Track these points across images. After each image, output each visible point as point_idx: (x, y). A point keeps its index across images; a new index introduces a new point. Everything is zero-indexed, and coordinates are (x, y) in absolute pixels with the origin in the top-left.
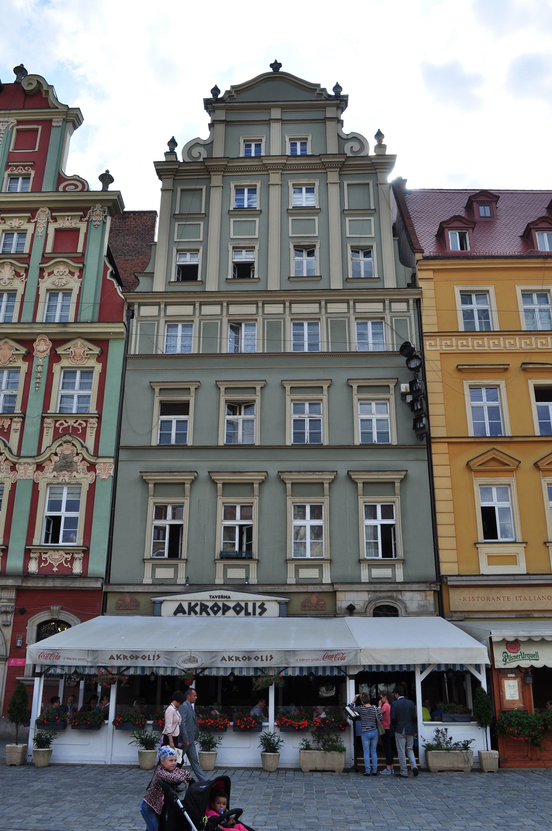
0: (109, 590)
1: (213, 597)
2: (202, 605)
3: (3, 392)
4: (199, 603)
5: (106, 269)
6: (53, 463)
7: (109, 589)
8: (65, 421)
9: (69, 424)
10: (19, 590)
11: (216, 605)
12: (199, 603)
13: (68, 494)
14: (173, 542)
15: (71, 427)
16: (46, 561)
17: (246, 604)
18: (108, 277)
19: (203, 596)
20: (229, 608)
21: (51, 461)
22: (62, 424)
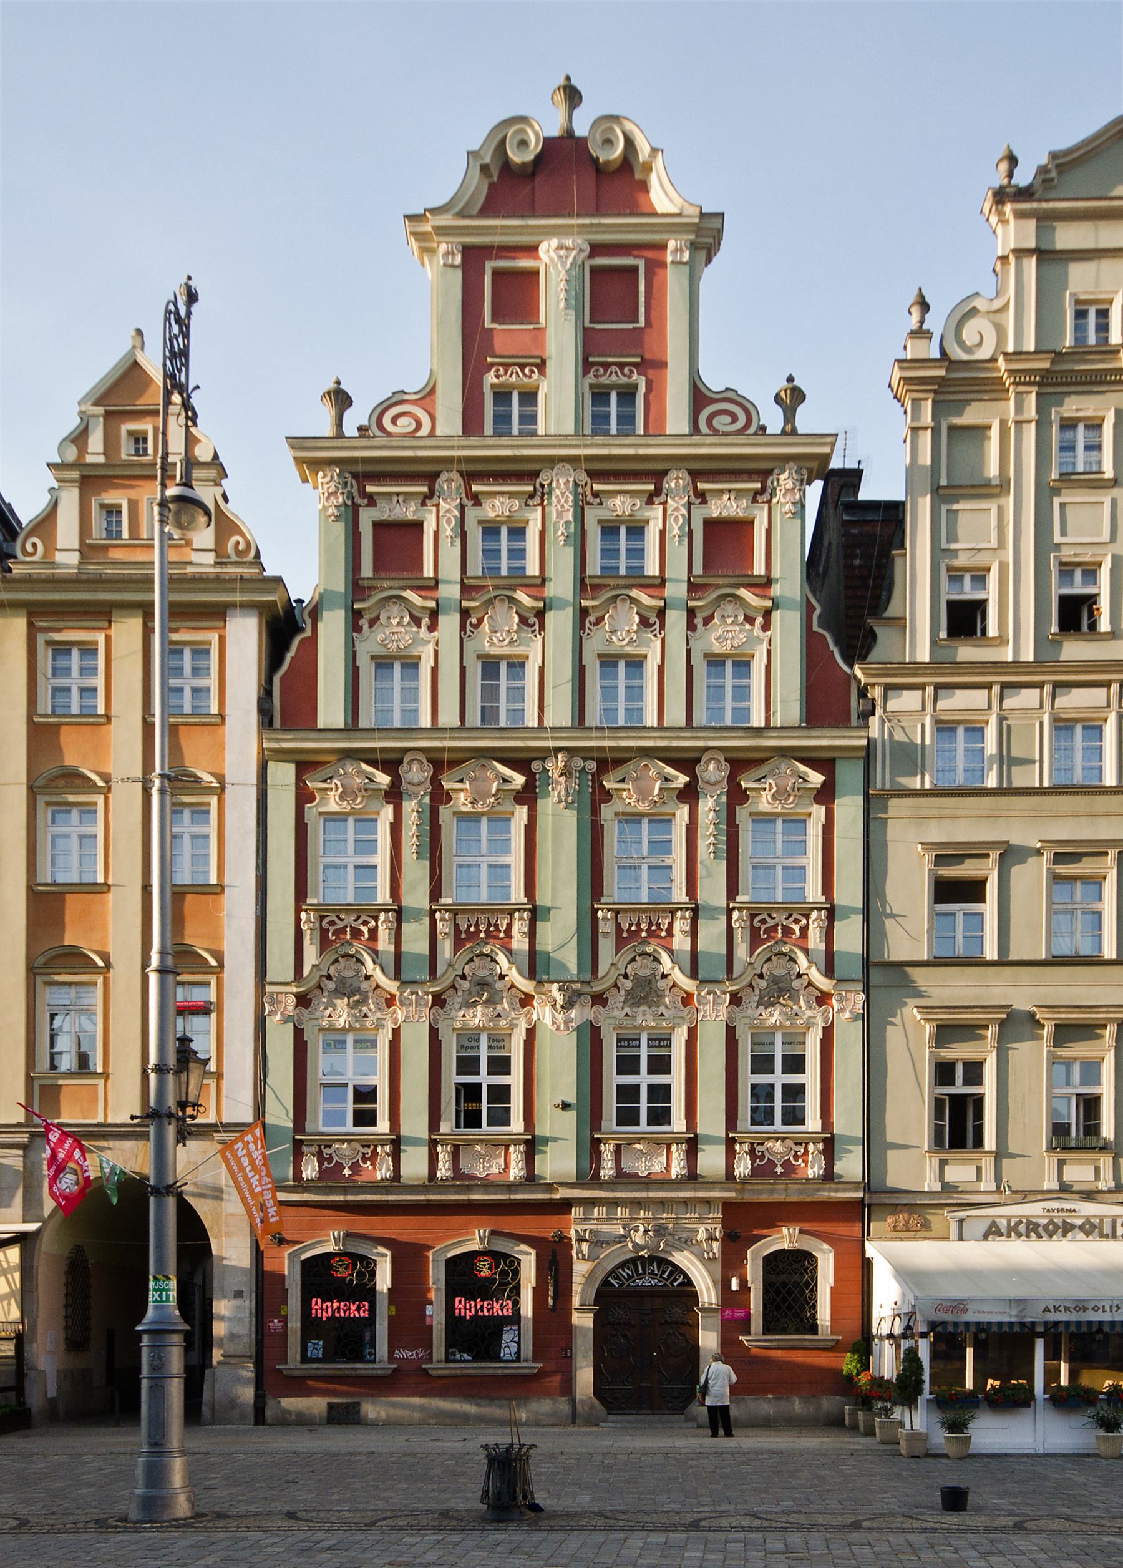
0: (876, 1201)
1: (1048, 1211)
2: (1029, 1223)
3: (646, 860)
4: (1024, 1220)
5: (810, 609)
6: (757, 992)
7: (876, 1199)
8: (770, 916)
9: (777, 920)
10: (728, 1206)
11: (1051, 1222)
12: (1024, 1220)
13: (783, 1043)
14: (958, 1124)
15: (779, 928)
16: (763, 1157)
17: (1101, 1221)
18: (815, 628)
19: (1033, 1210)
20: (1073, 1227)
21: (753, 988)
22: (763, 921)
